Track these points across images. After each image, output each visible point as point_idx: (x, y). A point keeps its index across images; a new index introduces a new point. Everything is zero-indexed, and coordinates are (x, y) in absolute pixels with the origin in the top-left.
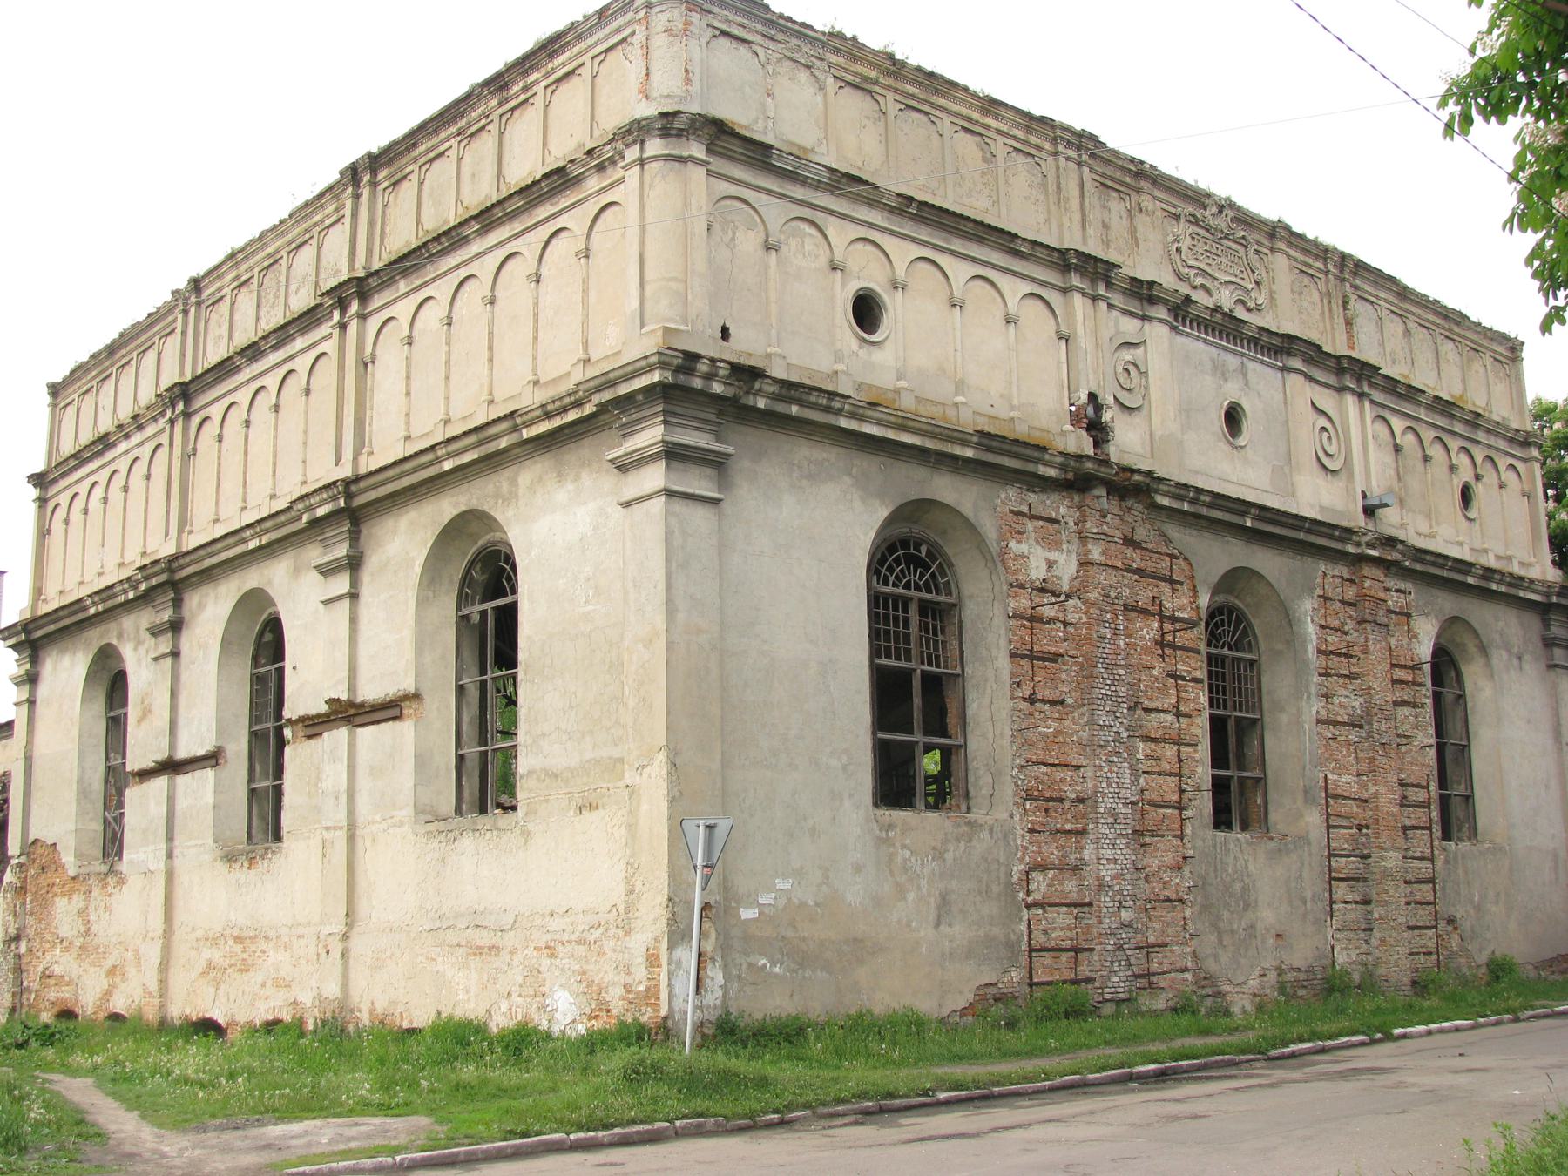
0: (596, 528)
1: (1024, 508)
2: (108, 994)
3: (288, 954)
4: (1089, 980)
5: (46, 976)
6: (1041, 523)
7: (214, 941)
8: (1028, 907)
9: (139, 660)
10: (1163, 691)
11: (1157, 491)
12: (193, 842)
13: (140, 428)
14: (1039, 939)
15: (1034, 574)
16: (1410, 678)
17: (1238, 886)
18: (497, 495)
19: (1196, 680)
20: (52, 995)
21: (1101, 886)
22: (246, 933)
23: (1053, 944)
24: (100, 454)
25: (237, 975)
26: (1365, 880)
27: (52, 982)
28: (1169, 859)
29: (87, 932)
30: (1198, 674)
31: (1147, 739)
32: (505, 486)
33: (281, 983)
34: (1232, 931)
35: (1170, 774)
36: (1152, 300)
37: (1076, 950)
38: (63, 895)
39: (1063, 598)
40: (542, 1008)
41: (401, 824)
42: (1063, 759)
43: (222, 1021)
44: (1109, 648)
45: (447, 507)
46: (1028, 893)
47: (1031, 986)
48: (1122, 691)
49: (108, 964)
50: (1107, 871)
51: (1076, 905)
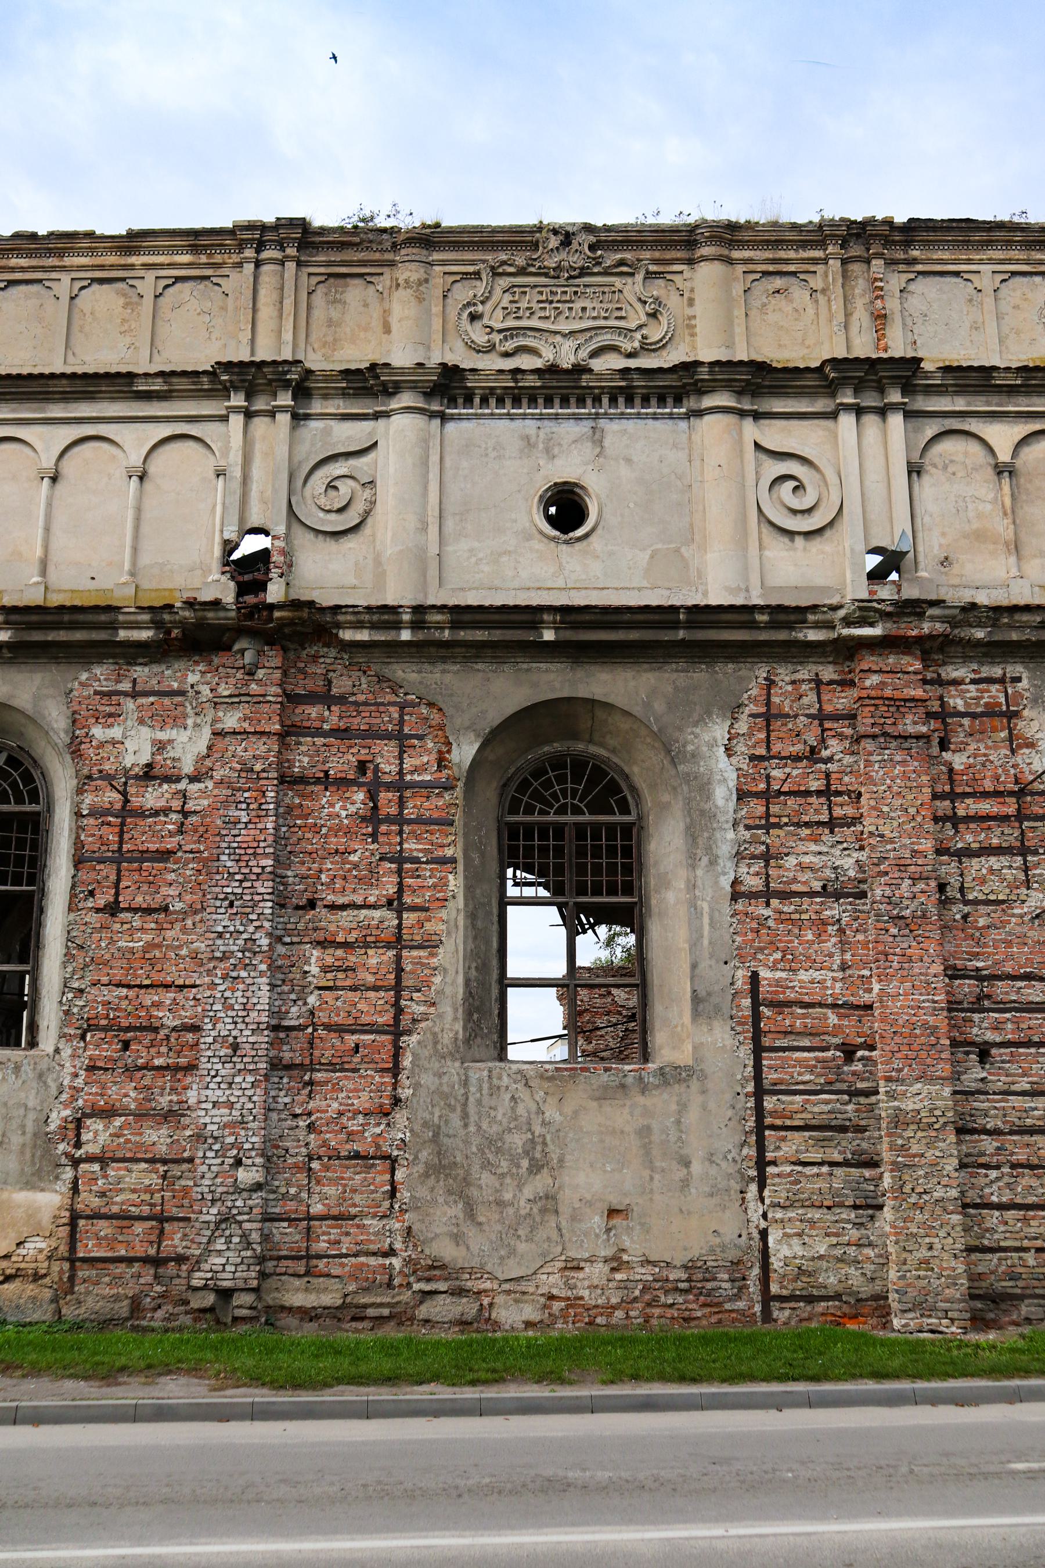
1: (126, 686)
4: (180, 1259)
6: (152, 699)
8: (76, 1163)
10: (371, 878)
11: (339, 626)
14: (89, 1200)
15: (128, 761)
16: (1011, 810)
17: (517, 1140)
19: (443, 861)
21: (200, 1137)
23: (115, 1209)
26: (861, 1130)
28: (363, 1101)
30: (449, 852)
31: (321, 944)
34: (500, 1203)
35: (376, 988)
36: (390, 390)
37: (162, 1219)
39: (185, 781)
42: (156, 977)
44: (245, 836)
46: (78, 1145)
47: (72, 1260)
48: (264, 887)
50: (212, 1119)
51: (165, 1162)
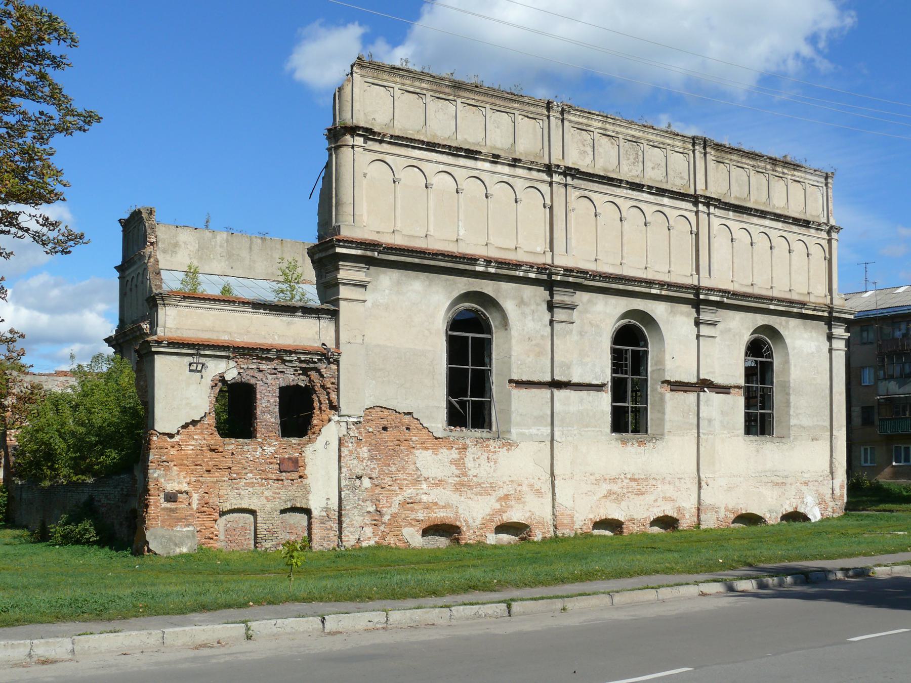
0: (818, 351)
3: (672, 487)
5: (408, 503)
7: (614, 480)
9: (523, 314)
12: (589, 429)
18: (781, 324)
20: (420, 516)
22: (636, 477)
29: (465, 474)
32: (784, 323)
33: (665, 499)
38: (426, 448)
40: (803, 502)
41: (738, 436)
43: (622, 519)
45: (762, 320)
49: (501, 493)
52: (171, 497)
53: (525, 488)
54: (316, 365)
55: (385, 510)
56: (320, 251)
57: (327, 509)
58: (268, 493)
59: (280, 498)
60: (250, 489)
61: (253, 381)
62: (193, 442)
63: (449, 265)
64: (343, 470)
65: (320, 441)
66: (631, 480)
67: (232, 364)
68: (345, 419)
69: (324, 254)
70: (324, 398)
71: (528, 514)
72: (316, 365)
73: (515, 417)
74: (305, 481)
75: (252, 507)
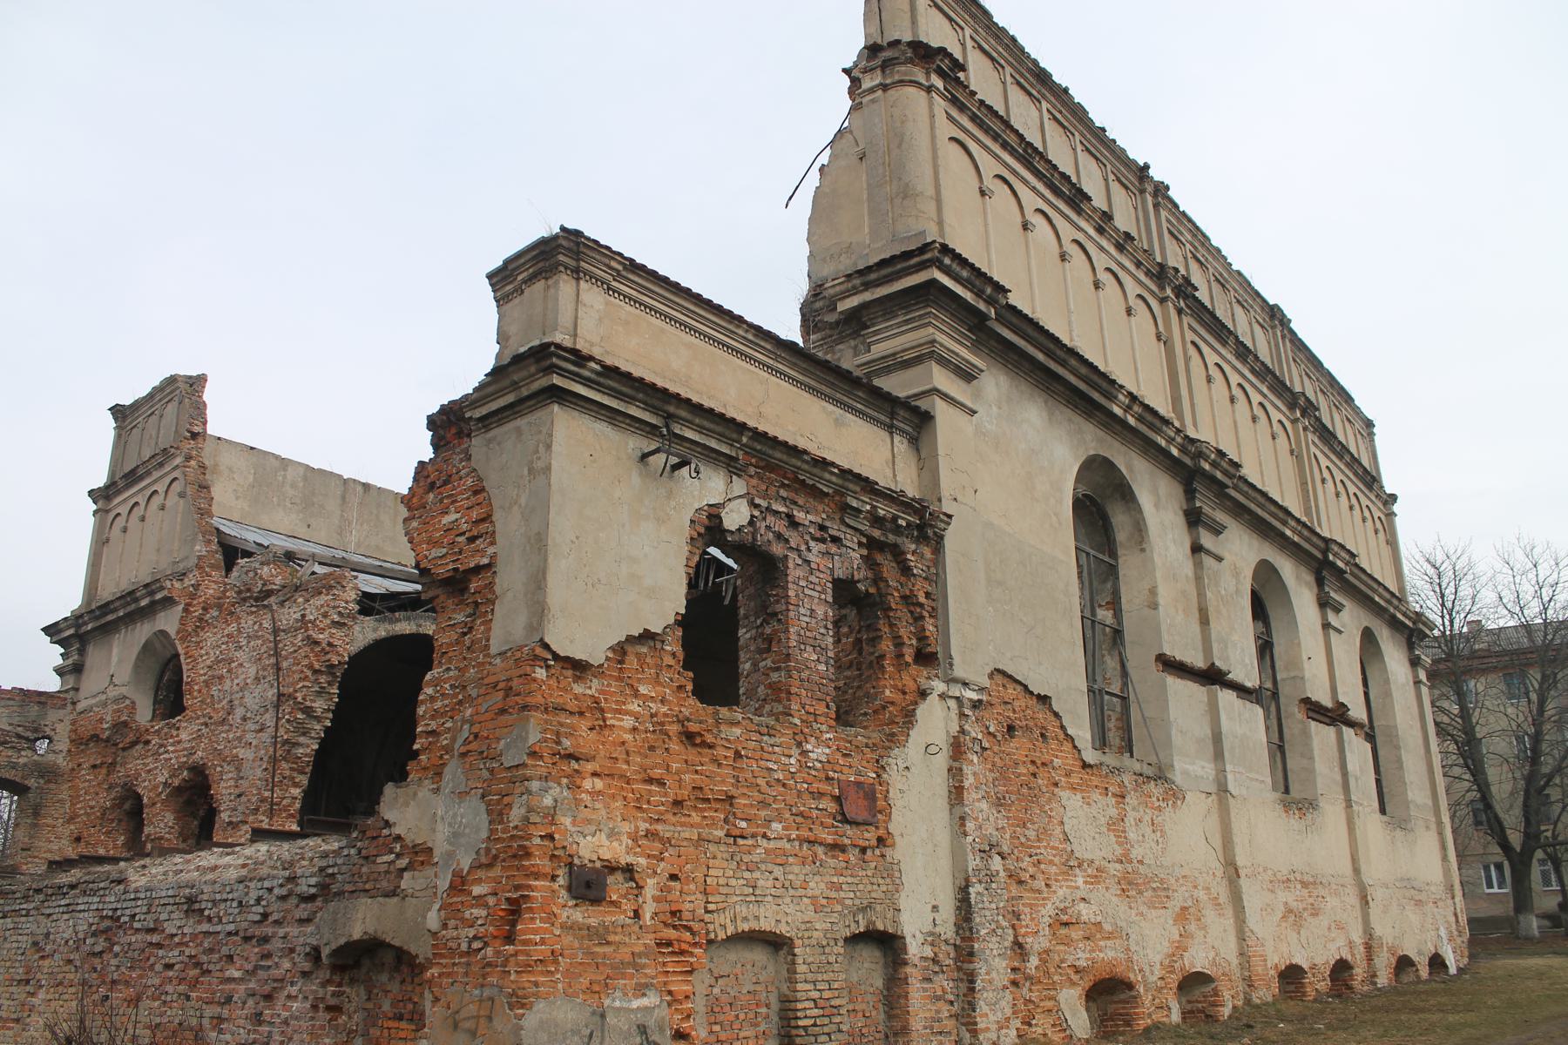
2: (1180, 948)
5: (1063, 923)
13: (1120, 248)
24: (1056, 191)
25: (1310, 919)
27: (1076, 933)
49: (1175, 904)
52: (588, 885)
53: (1201, 894)
54: (899, 540)
55: (1029, 940)
56: (867, 286)
57: (933, 939)
58: (817, 886)
59: (840, 901)
60: (778, 872)
61: (777, 549)
62: (634, 706)
63: (1082, 386)
64: (970, 826)
65: (917, 737)
66: (1305, 885)
67: (739, 486)
68: (956, 690)
69: (867, 296)
70: (905, 631)
71: (1212, 955)
72: (899, 540)
73: (1176, 738)
74: (888, 852)
75: (783, 929)
